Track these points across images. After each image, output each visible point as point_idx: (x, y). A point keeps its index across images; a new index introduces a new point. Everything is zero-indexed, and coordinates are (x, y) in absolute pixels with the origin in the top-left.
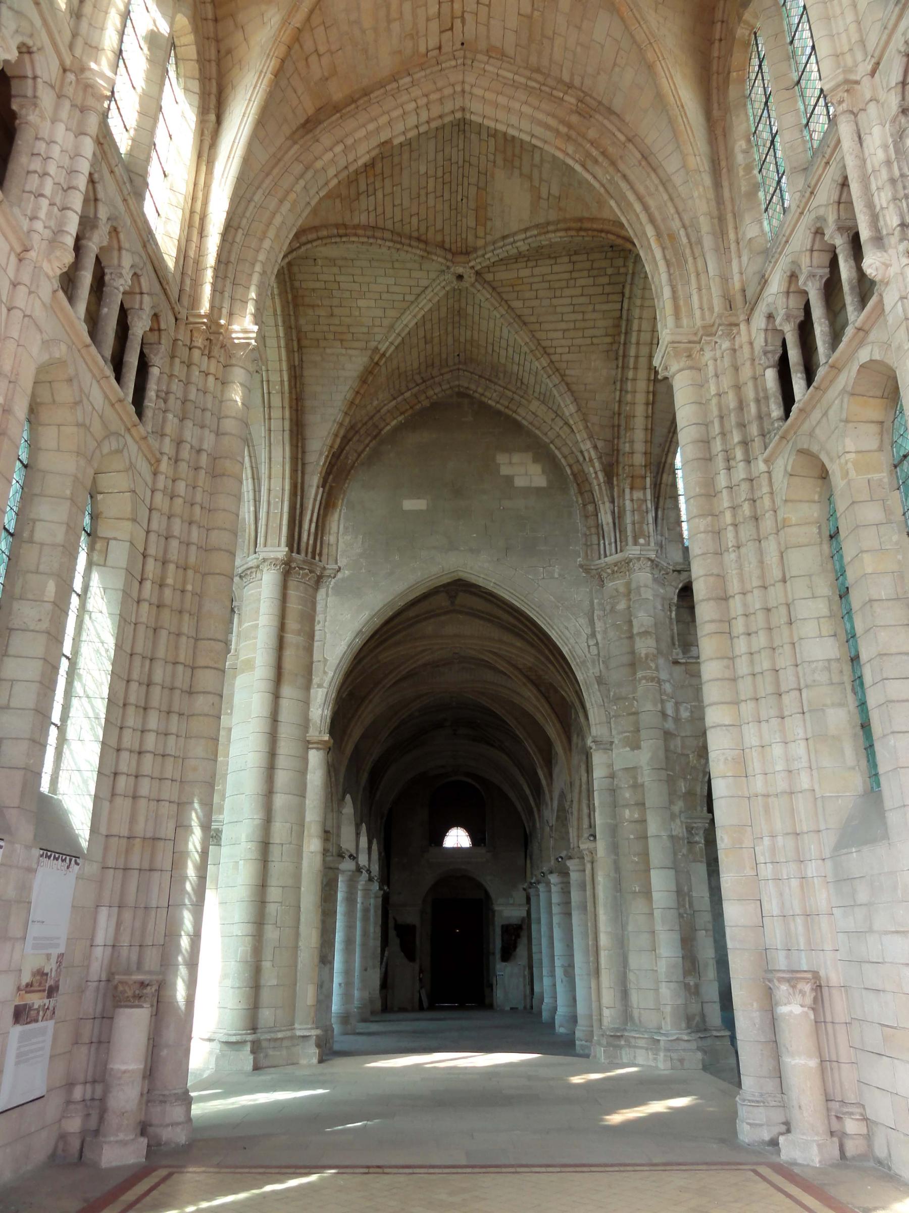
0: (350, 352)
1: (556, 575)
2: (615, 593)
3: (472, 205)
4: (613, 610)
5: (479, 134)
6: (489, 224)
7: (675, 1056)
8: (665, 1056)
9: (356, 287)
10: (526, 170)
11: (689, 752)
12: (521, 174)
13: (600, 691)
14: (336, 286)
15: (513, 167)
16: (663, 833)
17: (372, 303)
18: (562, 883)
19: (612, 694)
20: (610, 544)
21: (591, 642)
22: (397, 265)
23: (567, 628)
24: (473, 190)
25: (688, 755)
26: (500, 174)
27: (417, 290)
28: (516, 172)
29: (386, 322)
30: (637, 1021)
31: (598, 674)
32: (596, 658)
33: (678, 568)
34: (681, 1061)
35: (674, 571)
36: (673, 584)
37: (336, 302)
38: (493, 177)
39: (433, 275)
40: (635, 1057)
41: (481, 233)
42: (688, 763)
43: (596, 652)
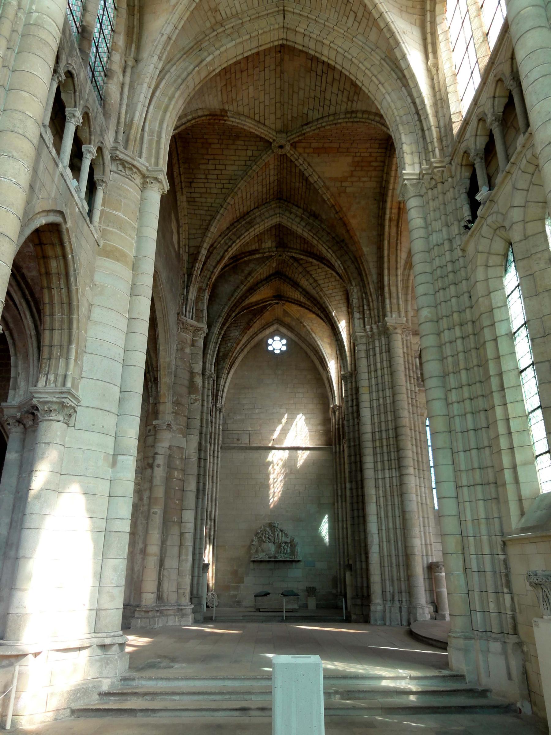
0: (219, 93)
2: (185, 341)
3: (326, 145)
4: (182, 349)
5: (370, 148)
6: (316, 155)
9: (262, 82)
10: (355, 173)
14: (261, 68)
15: (356, 167)
17: (251, 95)
19: (175, 399)
20: (190, 312)
22: (278, 105)
24: (336, 145)
26: (349, 159)
27: (262, 120)
28: (353, 169)
29: (240, 109)
30: (166, 600)
37: (251, 72)
39: (273, 126)
40: (167, 622)
41: (307, 151)
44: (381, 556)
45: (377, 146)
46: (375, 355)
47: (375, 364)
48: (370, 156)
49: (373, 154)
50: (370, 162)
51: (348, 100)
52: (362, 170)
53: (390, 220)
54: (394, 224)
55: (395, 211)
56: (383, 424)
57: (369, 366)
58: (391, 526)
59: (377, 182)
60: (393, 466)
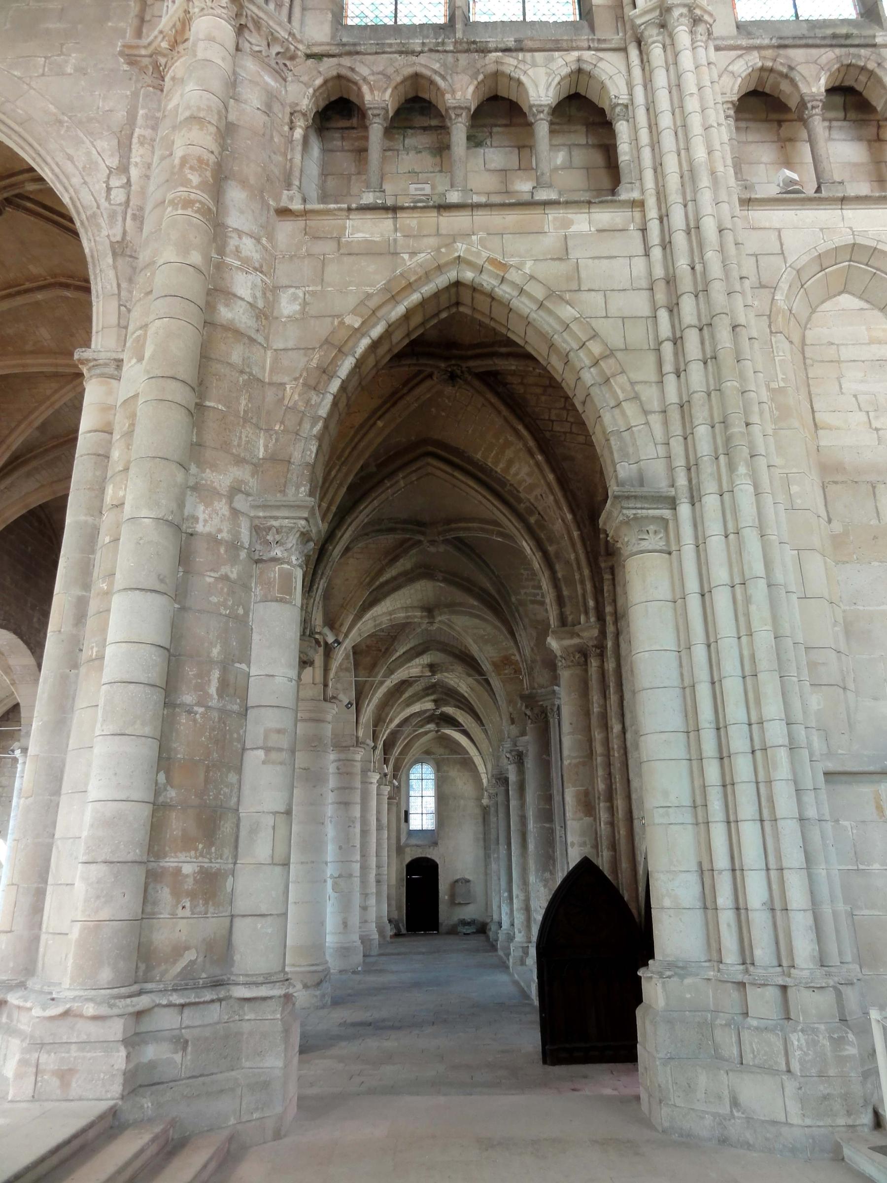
1: (69, 69)
7: (49, 1061)
8: (23, 1062)
11: (286, 379)
13: (115, 267)
16: (144, 513)
18: (340, 760)
21: (115, 182)
23: (70, 158)
25: (283, 385)
31: (119, 238)
32: (120, 209)
33: (316, 50)
34: (64, 1076)
35: (309, 56)
36: (305, 78)
42: (283, 398)
43: (118, 196)
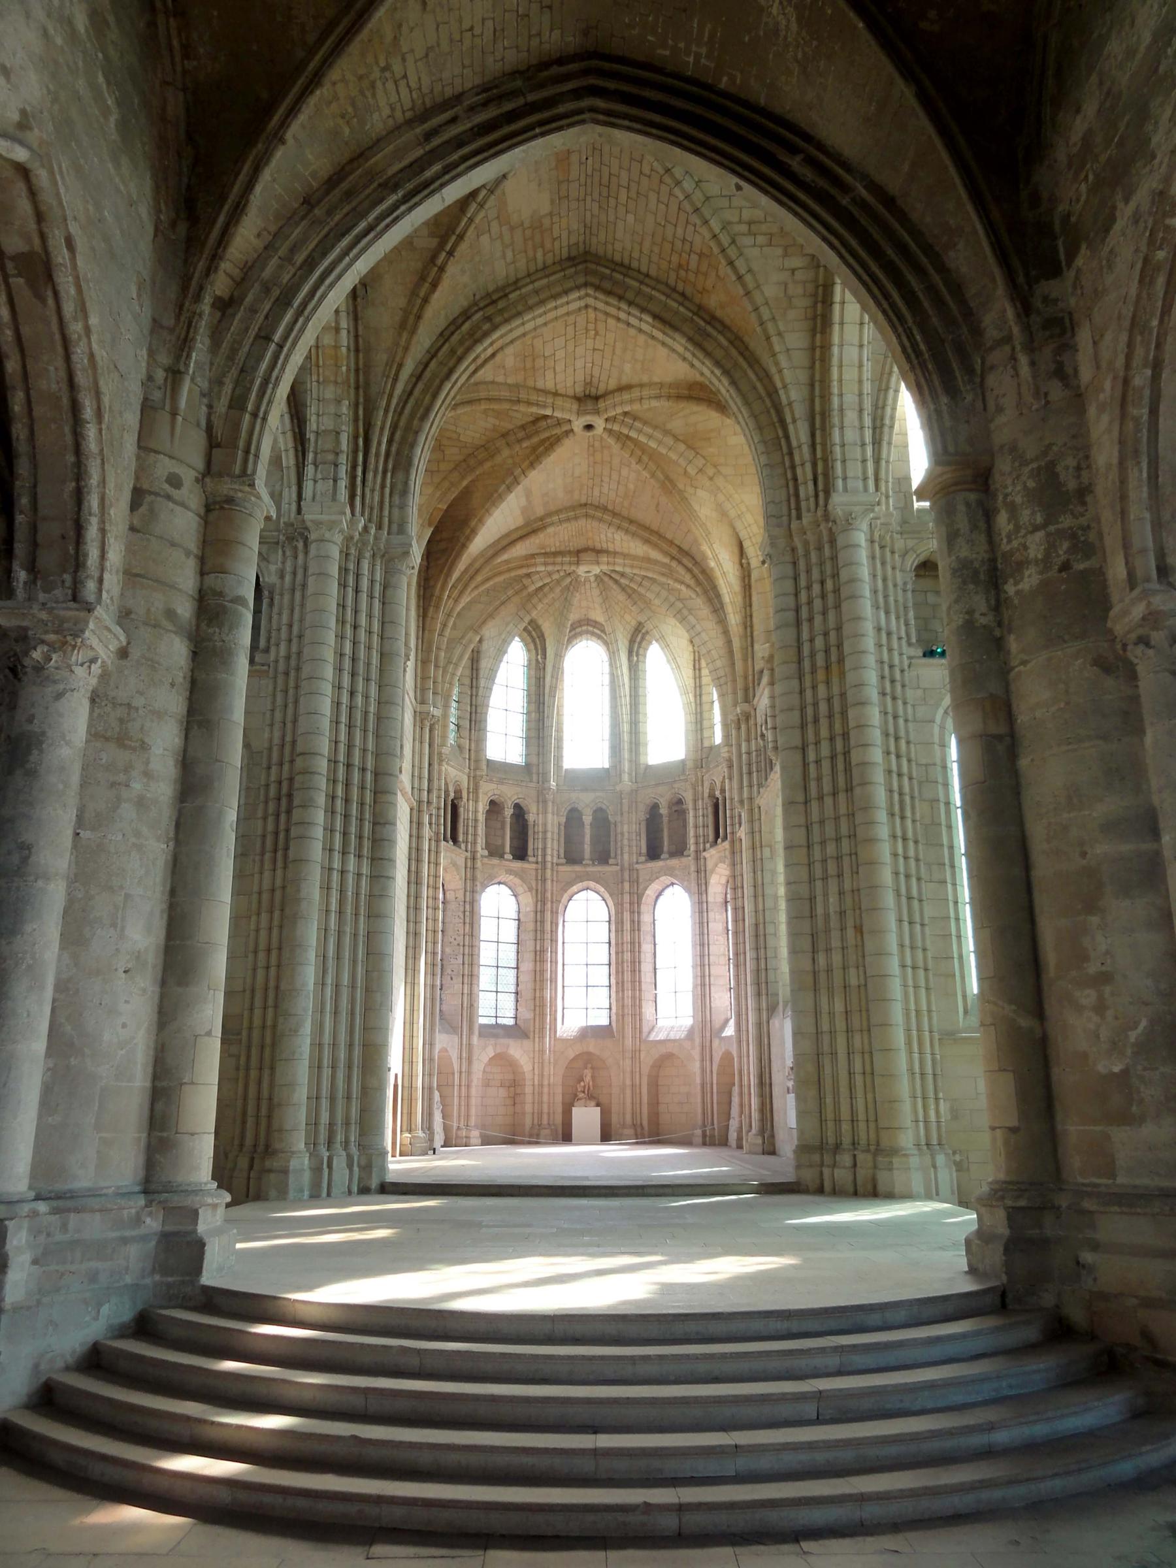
12: (522, 224)
28: (526, 225)
38: (552, 202)
44: (318, 1046)
45: (573, 240)
46: (357, 591)
47: (356, 612)
48: (554, 239)
49: (557, 244)
50: (542, 246)
51: (750, 223)
52: (525, 240)
53: (474, 360)
54: (472, 368)
55: (490, 351)
56: (357, 753)
57: (342, 606)
58: (345, 979)
59: (507, 276)
60: (365, 852)
